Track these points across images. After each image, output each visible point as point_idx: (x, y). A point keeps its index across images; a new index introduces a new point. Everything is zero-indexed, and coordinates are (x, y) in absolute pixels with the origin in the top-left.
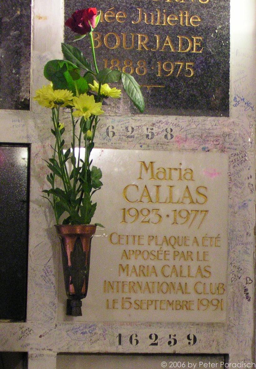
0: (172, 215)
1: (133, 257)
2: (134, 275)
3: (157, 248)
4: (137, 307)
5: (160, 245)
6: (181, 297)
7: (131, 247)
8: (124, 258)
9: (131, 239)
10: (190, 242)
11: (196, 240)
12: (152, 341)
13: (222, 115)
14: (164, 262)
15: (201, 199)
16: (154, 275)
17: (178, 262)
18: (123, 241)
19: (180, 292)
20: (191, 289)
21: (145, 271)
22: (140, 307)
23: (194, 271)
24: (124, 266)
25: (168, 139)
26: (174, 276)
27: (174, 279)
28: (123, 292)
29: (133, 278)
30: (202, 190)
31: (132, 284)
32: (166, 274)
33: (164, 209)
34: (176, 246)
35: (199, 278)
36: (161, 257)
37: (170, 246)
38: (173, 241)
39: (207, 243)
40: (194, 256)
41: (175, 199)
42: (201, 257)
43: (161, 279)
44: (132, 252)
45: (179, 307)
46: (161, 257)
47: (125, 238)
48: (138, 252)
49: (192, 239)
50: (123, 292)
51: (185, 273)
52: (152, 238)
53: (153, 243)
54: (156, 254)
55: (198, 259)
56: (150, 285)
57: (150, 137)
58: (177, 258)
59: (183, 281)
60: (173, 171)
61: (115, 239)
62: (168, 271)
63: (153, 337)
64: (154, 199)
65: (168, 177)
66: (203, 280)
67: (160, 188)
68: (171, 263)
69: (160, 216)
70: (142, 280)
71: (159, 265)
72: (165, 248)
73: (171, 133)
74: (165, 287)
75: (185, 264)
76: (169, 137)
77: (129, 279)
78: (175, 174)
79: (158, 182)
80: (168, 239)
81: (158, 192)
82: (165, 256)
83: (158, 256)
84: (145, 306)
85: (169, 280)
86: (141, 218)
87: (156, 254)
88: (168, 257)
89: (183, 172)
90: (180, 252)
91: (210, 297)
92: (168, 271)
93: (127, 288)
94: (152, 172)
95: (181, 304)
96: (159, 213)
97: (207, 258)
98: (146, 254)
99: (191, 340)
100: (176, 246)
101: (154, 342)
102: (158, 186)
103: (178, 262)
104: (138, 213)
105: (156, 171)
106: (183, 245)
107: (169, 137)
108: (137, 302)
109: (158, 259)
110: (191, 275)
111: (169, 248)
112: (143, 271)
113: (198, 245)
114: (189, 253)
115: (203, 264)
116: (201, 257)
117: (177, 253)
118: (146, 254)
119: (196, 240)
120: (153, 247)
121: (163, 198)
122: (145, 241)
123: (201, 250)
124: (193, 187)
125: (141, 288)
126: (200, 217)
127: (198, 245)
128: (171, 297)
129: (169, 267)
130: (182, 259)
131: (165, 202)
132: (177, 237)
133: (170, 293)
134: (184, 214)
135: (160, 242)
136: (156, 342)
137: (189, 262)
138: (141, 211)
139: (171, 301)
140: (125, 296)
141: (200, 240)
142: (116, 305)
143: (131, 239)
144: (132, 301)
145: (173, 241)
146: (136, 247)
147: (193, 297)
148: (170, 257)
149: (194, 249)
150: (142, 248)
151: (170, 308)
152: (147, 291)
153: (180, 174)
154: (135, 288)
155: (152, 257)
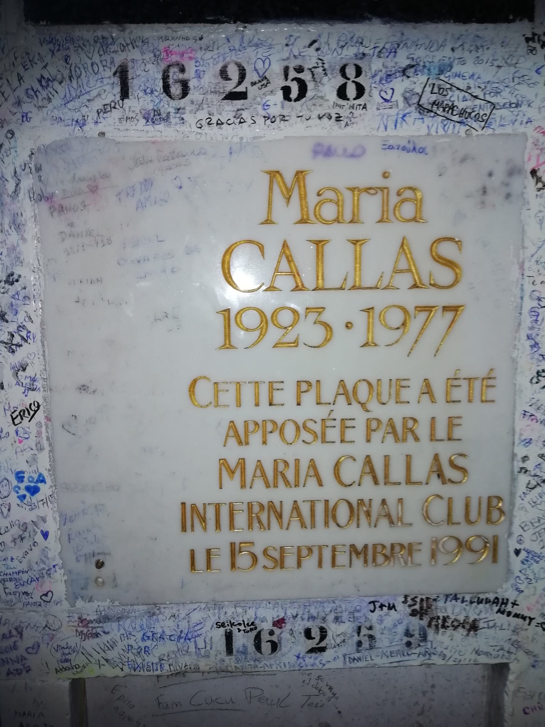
0: (360, 320)
1: (256, 438)
2: (259, 483)
3: (321, 412)
4: (270, 564)
5: (330, 404)
6: (384, 534)
7: (248, 412)
8: (232, 442)
9: (248, 393)
10: (411, 394)
11: (428, 390)
12: (312, 644)
13: (511, 17)
14: (338, 450)
15: (444, 275)
16: (312, 482)
17: (379, 448)
18: (228, 398)
19: (384, 523)
20: (412, 513)
21: (290, 474)
22: (280, 563)
23: (421, 469)
24: (233, 463)
25: (348, 99)
26: (368, 479)
27: (368, 491)
28: (232, 526)
29: (260, 493)
30: (447, 250)
31: (256, 509)
32: (347, 479)
33: (341, 307)
34: (373, 405)
35: (436, 485)
36: (333, 434)
37: (356, 406)
38: (363, 392)
39: (460, 393)
40: (423, 431)
41: (369, 280)
42: (441, 432)
43: (331, 491)
44: (251, 427)
45: (380, 559)
46: (333, 434)
47: (232, 389)
48: (270, 427)
49: (416, 385)
50: (232, 526)
51: (398, 472)
52: (303, 387)
53: (309, 399)
54: (317, 428)
55: (433, 438)
56: (305, 509)
57: (294, 94)
58: (376, 437)
59: (391, 494)
60: (365, 197)
61: (204, 391)
62: (351, 471)
63: (316, 633)
64: (308, 277)
65: (348, 216)
66: (448, 491)
67: (328, 249)
68: (360, 449)
69: (327, 326)
70: (284, 496)
71: (325, 456)
72: (342, 410)
73: (357, 80)
74: (343, 513)
75: (397, 451)
76: (351, 91)
77: (248, 495)
78: (371, 206)
79: (318, 231)
80: (350, 387)
81: (320, 255)
82: (343, 434)
83: (324, 434)
84: (291, 560)
85: (353, 495)
86: (274, 334)
87: (317, 428)
88: (350, 434)
89: (394, 199)
90: (385, 420)
91: (464, 532)
92: (351, 471)
93: (241, 519)
94: (303, 198)
95: (387, 552)
96: (326, 317)
97: (457, 433)
98: (290, 431)
99: (412, 636)
100: (373, 405)
101: (317, 644)
102: (319, 244)
103: (379, 448)
104: (267, 323)
105: (312, 199)
106: (393, 400)
107: (351, 91)
108: (272, 553)
109: (324, 441)
110: (415, 477)
111: (355, 411)
112: (279, 474)
113: (433, 400)
114: (410, 424)
115: (446, 451)
116: (441, 432)
117: (374, 425)
118: (290, 431)
119: (428, 390)
120: (310, 410)
121: (334, 278)
122: (287, 395)
123: (442, 412)
124: (420, 238)
125: (280, 516)
126: (440, 321)
127: (433, 400)
128: (362, 535)
129: (355, 460)
130: (390, 438)
131: (341, 288)
132: (374, 383)
133: (358, 526)
134: (395, 318)
135: (328, 395)
136: (322, 645)
137: (410, 446)
138: (275, 313)
139: (360, 547)
140: (237, 536)
141: (439, 389)
142: (215, 562)
143: (248, 393)
144: (258, 550)
145: (363, 392)
146: (264, 413)
147: (419, 533)
148: (357, 434)
149: (423, 411)
150: (278, 415)
151: (358, 563)
152: (295, 523)
153: (385, 203)
154: (264, 517)
155: (308, 437)
